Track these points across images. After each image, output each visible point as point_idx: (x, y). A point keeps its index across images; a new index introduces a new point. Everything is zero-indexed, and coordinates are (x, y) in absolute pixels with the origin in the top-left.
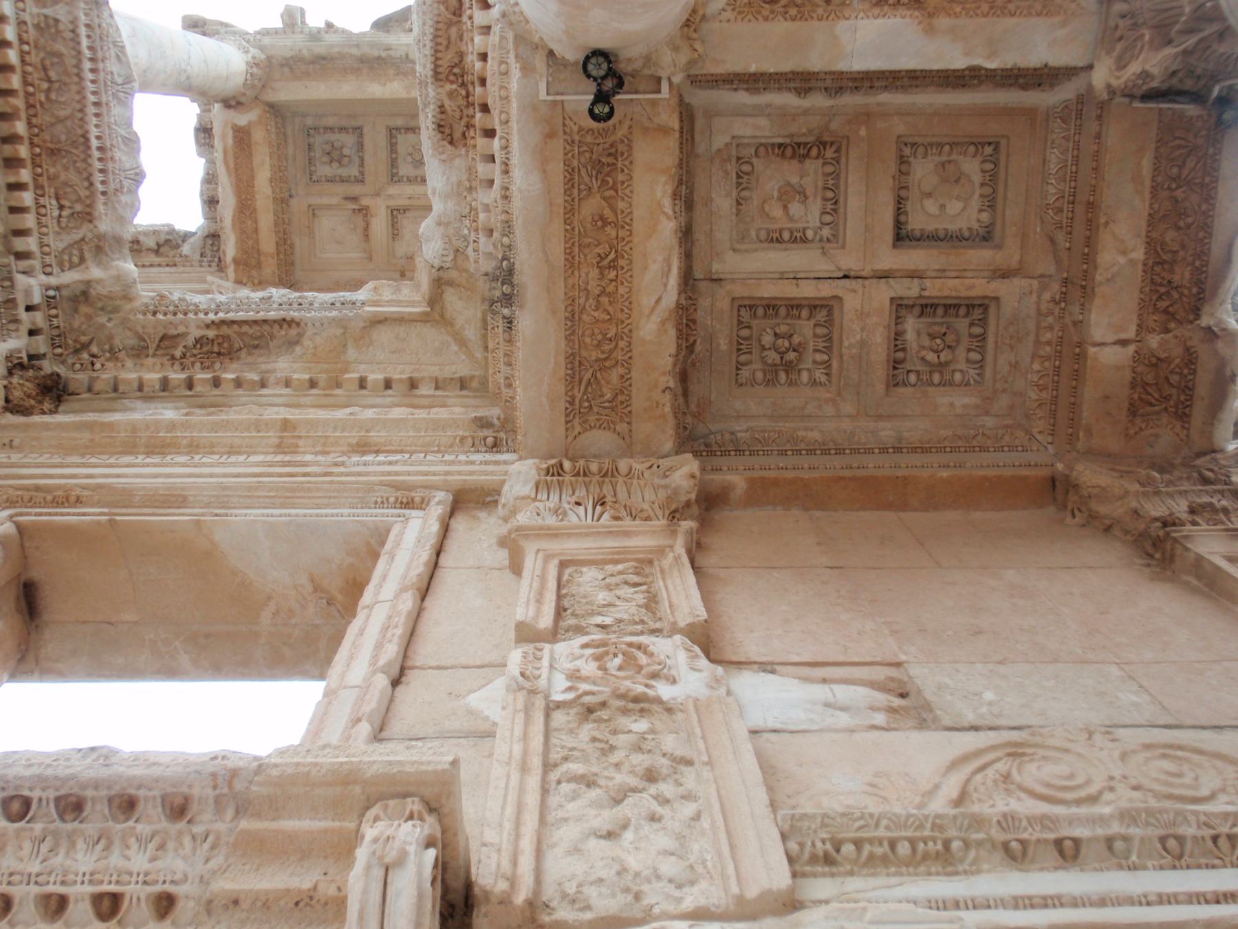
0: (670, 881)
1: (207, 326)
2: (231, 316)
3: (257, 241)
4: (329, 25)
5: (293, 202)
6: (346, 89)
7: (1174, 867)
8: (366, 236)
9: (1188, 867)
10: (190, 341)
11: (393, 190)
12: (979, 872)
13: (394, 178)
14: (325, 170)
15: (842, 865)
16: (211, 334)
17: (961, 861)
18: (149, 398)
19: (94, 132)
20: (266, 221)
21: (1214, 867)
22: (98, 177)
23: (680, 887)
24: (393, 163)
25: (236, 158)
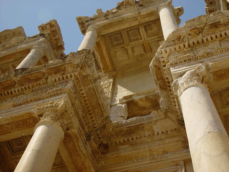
1: (127, 128)
2: (131, 126)
3: (106, 63)
4: (108, 11)
5: (111, 52)
6: (117, 29)
8: (127, 54)
10: (125, 131)
11: (131, 44)
13: (130, 41)
14: (115, 43)
16: (128, 129)
18: (122, 145)
19: (100, 102)
20: (107, 59)
22: (103, 109)
24: (129, 38)
25: (98, 48)
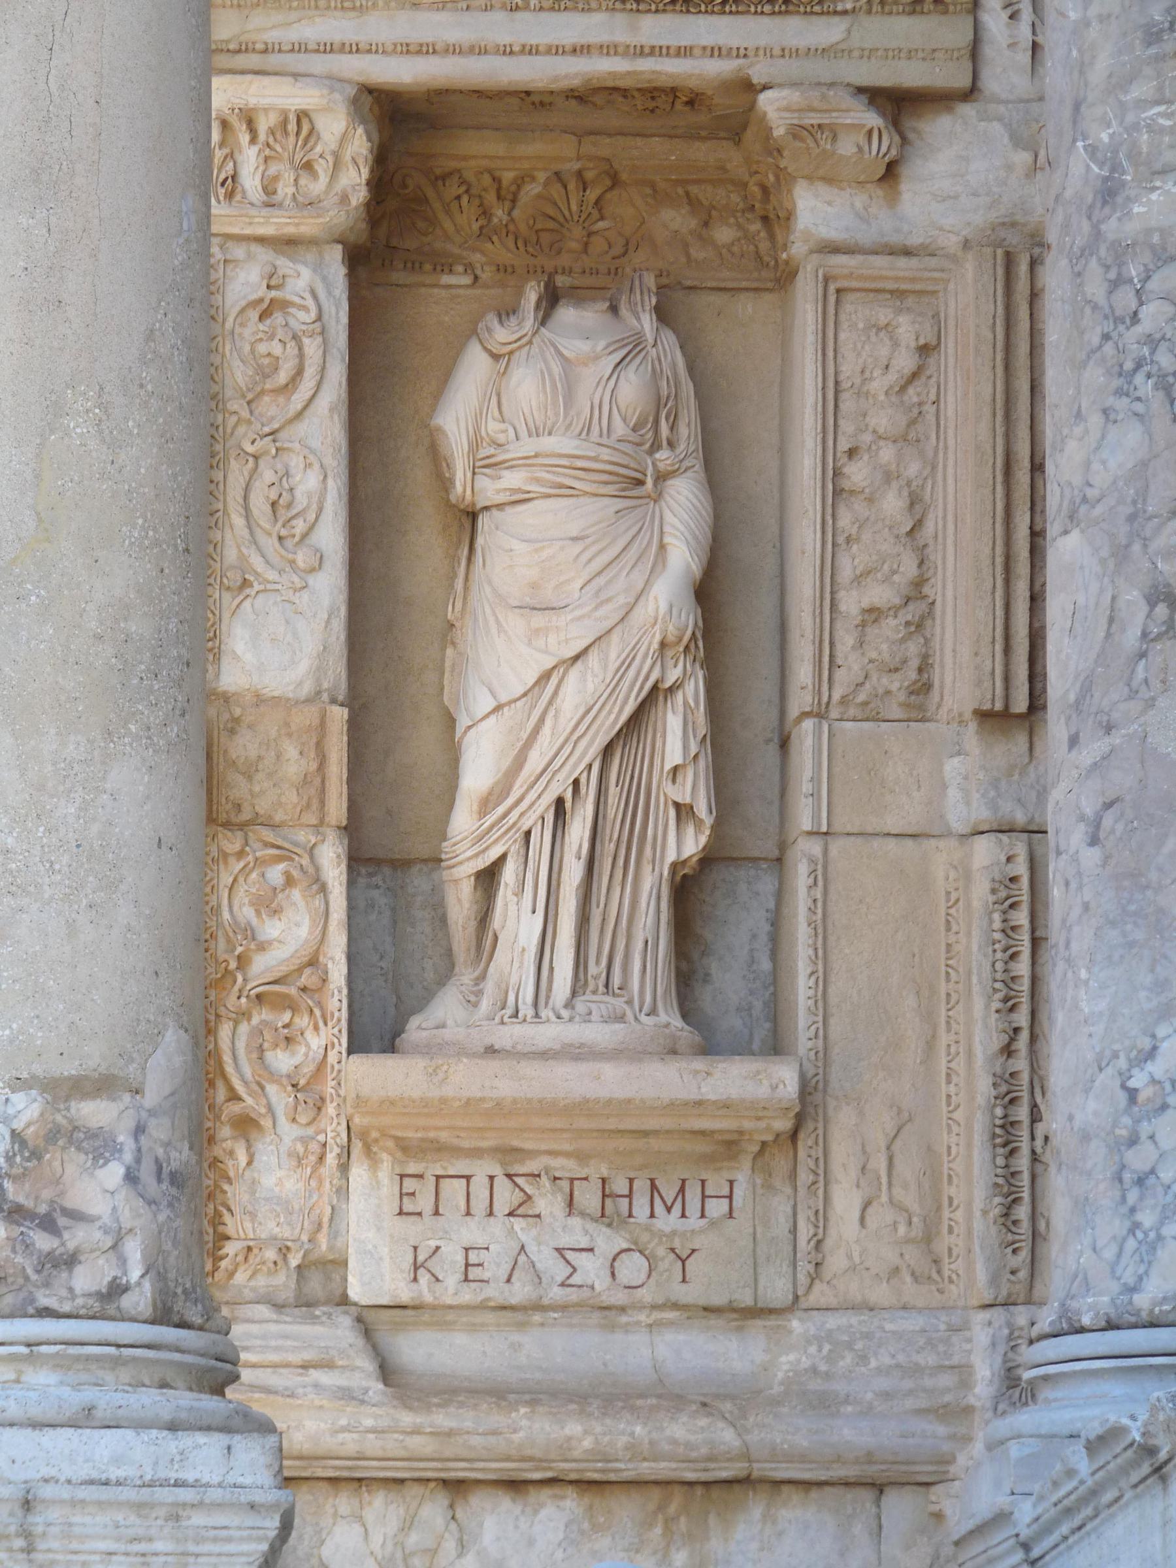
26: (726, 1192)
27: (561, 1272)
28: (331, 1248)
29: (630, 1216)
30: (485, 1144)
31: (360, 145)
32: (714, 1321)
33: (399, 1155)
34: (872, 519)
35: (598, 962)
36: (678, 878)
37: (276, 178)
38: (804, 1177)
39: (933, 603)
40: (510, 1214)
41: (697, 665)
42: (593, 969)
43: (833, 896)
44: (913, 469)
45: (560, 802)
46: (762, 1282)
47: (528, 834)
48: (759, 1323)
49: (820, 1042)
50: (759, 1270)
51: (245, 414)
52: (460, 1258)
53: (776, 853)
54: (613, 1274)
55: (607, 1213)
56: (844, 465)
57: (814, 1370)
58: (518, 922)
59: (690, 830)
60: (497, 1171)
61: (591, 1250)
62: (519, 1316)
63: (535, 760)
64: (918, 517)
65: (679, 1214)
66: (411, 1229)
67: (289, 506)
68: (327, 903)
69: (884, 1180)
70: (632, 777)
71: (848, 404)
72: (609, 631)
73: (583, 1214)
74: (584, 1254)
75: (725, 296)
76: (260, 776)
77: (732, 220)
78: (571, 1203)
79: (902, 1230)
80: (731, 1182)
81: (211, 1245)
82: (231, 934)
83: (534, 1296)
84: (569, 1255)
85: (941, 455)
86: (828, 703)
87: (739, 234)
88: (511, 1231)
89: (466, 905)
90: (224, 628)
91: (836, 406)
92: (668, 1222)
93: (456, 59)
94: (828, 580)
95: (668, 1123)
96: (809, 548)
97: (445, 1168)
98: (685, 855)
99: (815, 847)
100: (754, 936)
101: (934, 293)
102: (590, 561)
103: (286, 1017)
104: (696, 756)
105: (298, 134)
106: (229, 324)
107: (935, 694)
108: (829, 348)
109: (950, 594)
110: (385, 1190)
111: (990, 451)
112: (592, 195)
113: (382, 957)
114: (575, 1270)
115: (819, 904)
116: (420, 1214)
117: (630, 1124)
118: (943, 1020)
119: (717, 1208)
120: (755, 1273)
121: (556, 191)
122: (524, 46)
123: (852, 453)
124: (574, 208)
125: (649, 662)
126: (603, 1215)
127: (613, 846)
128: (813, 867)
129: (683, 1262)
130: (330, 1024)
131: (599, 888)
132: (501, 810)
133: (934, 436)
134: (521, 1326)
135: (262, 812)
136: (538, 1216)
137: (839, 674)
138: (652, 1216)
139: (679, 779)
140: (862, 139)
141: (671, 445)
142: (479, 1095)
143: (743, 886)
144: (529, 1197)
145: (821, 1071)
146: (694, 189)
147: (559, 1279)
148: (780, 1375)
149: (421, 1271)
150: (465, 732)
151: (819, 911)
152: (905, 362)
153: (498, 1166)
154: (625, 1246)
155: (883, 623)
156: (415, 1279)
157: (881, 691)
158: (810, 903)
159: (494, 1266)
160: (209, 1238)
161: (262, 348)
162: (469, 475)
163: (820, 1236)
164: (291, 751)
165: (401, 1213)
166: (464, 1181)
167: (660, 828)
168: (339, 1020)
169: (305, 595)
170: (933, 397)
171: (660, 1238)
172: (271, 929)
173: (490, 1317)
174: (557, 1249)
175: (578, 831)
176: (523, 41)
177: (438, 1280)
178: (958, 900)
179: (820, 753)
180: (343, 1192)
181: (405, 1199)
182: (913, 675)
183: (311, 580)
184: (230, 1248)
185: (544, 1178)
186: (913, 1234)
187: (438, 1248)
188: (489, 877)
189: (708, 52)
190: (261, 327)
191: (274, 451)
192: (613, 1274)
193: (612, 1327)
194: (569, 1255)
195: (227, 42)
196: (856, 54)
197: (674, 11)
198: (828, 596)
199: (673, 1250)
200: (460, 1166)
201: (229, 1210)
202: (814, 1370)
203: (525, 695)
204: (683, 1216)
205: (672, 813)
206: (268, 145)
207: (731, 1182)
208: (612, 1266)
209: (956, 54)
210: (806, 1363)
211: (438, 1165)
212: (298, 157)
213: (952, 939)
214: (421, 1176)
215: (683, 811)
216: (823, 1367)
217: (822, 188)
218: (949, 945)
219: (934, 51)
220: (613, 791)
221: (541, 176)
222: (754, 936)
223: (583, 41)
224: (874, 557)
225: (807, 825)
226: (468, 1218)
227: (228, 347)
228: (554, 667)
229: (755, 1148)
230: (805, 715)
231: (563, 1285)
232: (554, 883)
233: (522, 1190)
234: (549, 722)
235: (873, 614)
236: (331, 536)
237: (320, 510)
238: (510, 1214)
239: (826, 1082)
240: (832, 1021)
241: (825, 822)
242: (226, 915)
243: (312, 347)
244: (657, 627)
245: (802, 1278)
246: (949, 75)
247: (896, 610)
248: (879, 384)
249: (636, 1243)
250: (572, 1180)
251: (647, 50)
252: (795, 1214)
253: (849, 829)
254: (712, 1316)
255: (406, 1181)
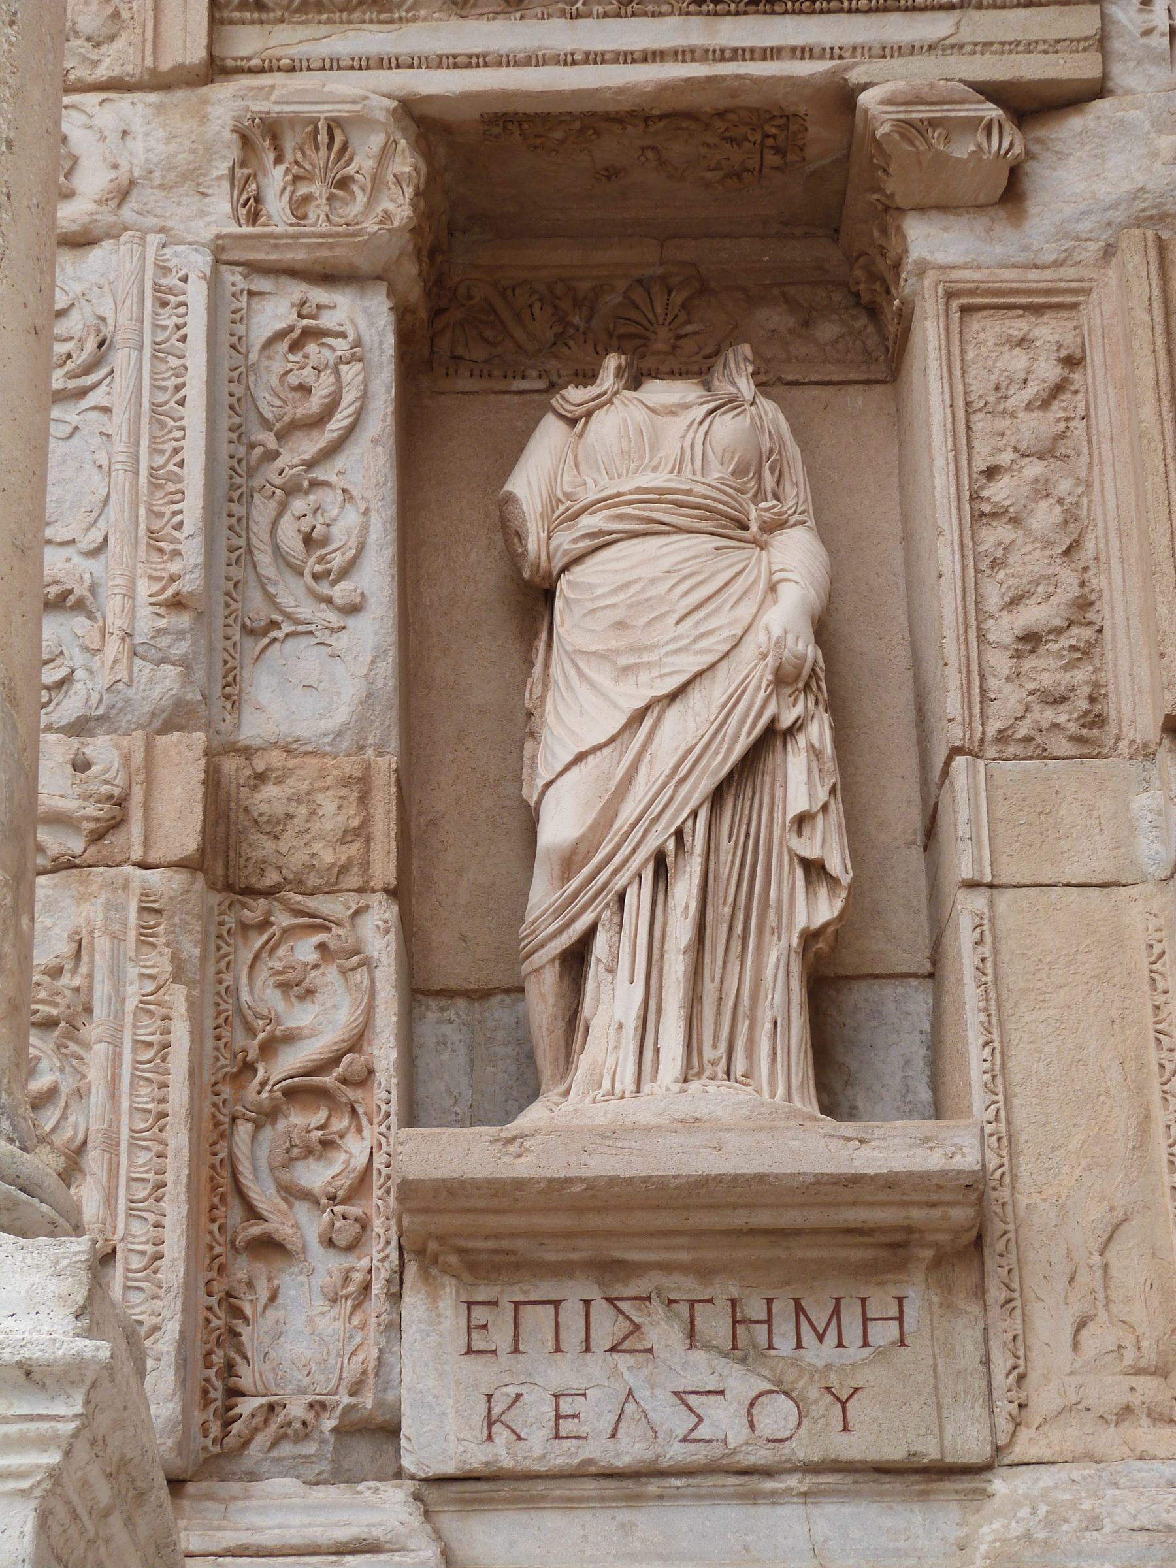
0: (88, 39)
7: (619, 15)
9: (633, 15)
12: (414, 19)
15: (273, 11)
17: (399, 7)
21: (660, 14)
23: (98, 45)
26: (894, 1312)
27: (681, 1423)
28: (379, 1404)
29: (771, 1347)
30: (575, 1256)
31: (405, 163)
32: (890, 1484)
33: (466, 1276)
34: (1019, 541)
35: (715, 1046)
36: (811, 955)
37: (307, 199)
38: (996, 1294)
39: (1100, 631)
40: (613, 1350)
41: (821, 708)
42: (709, 1054)
43: (1005, 956)
44: (1064, 486)
45: (660, 859)
46: (949, 1427)
47: (621, 897)
48: (948, 1485)
49: (1003, 1127)
50: (945, 1414)
51: (271, 442)
52: (548, 1409)
53: (927, 967)
54: (752, 1425)
55: (740, 1345)
56: (982, 488)
57: (1028, 1537)
58: (613, 1000)
59: (823, 892)
60: (594, 1293)
61: (722, 1392)
62: (630, 1486)
63: (629, 811)
64: (1075, 536)
65: (835, 1342)
66: (484, 1373)
67: (324, 542)
68: (373, 981)
69: (1100, 1295)
70: (748, 834)
71: (981, 423)
72: (712, 667)
73: (709, 1347)
74: (712, 1398)
75: (831, 390)
76: (286, 836)
77: (835, 317)
78: (691, 1334)
79: (1129, 1357)
80: (900, 1300)
81: (219, 1403)
82: (250, 1018)
83: (648, 1455)
84: (692, 1400)
85: (1096, 469)
86: (982, 740)
87: (843, 330)
88: (614, 1372)
89: (551, 1000)
90: (246, 674)
91: (968, 428)
92: (819, 1353)
93: (512, 71)
94: (971, 607)
95: (814, 1217)
96: (946, 570)
97: (525, 1292)
98: (817, 923)
99: (978, 901)
100: (907, 1062)
101: (1074, 306)
102: (685, 594)
103: (323, 1114)
104: (825, 808)
105: (330, 147)
106: (253, 356)
107: (1112, 729)
108: (956, 366)
109: (1120, 615)
110: (447, 1324)
111: (1157, 437)
112: (678, 298)
113: (456, 1101)
114: (701, 1420)
115: (989, 963)
116: (494, 1352)
117: (763, 1219)
118: (1157, 1096)
119: (882, 1334)
120: (940, 1416)
121: (638, 295)
122: (587, 54)
123: (991, 472)
124: (659, 310)
125: (762, 695)
126: (735, 1348)
127: (727, 910)
128: (977, 921)
129: (844, 1404)
130: (376, 1121)
131: (713, 961)
132: (586, 871)
133: (1086, 451)
134: (634, 1499)
135: (291, 876)
136: (650, 1351)
137: (992, 709)
138: (799, 1346)
139: (807, 830)
140: (981, 137)
141: (776, 497)
142: (563, 1174)
143: (890, 1006)
144: (637, 1327)
145: (1006, 1161)
146: (791, 290)
147: (680, 1433)
148: (983, 1548)
149: (497, 1428)
150: (542, 794)
151: (989, 971)
152: (1048, 371)
153: (596, 1288)
154: (765, 1386)
155: (1041, 650)
156: (490, 1438)
157: (1045, 725)
158: (977, 961)
159: (595, 1414)
160: (217, 1394)
161: (293, 379)
162: (544, 536)
163: (1021, 1370)
164: (328, 803)
165: (469, 1351)
166: (551, 1308)
167: (786, 890)
168: (388, 1115)
169: (344, 635)
170: (1081, 411)
171: (812, 1375)
172: (301, 1017)
173: (589, 1487)
174: (676, 1393)
175: (684, 890)
176: (586, 48)
177: (519, 1438)
178: (1163, 954)
179: (977, 795)
180: (394, 1327)
181: (475, 1335)
182: (1084, 705)
183: (351, 622)
184: (247, 1406)
185: (655, 1301)
186: (1143, 1363)
187: (519, 1396)
188: (576, 959)
189: (798, 53)
190: (291, 357)
191: (306, 484)
192: (752, 1425)
193: (753, 1497)
194: (692, 1400)
195: (249, 59)
196: (968, 48)
197: (757, 12)
198: (973, 623)
199: (828, 1389)
200: (546, 1289)
201: (246, 1358)
202: (1028, 1537)
203: (613, 739)
204: (840, 1344)
205: (799, 873)
206: (296, 163)
207: (900, 1300)
208: (749, 1413)
209: (1082, 45)
210: (1016, 1530)
211: (516, 1288)
212: (330, 175)
213: (1160, 999)
214: (494, 1304)
215: (814, 869)
216: (1041, 1535)
217: (935, 216)
218: (1157, 1008)
219: (1058, 41)
220: (726, 846)
221: (621, 285)
222: (907, 1062)
223: (655, 46)
224: (1025, 580)
225: (967, 874)
226: (558, 1356)
227: (252, 378)
228: (647, 708)
229: (929, 1253)
230: (956, 751)
231: (685, 1440)
232: (656, 951)
233: (628, 1318)
234: (643, 770)
235: (1031, 640)
236: (376, 579)
237: (361, 548)
238: (613, 1350)
239: (1014, 1178)
240: (1016, 1101)
241: (988, 870)
242: (245, 996)
243: (349, 372)
244: (769, 658)
245: (1004, 1425)
246: (1077, 67)
247: (1058, 632)
248: (1019, 398)
249: (779, 1383)
250: (692, 1303)
251: (727, 54)
252: (987, 1341)
253: (1019, 880)
254: (886, 1478)
255: (477, 1311)
